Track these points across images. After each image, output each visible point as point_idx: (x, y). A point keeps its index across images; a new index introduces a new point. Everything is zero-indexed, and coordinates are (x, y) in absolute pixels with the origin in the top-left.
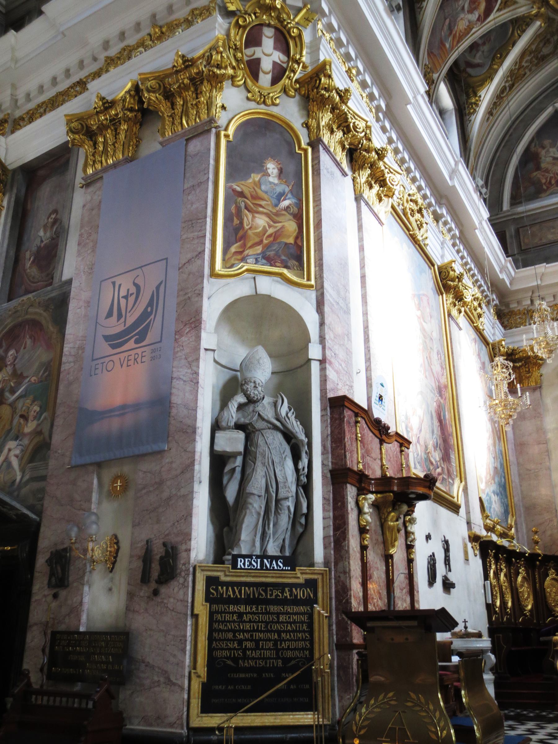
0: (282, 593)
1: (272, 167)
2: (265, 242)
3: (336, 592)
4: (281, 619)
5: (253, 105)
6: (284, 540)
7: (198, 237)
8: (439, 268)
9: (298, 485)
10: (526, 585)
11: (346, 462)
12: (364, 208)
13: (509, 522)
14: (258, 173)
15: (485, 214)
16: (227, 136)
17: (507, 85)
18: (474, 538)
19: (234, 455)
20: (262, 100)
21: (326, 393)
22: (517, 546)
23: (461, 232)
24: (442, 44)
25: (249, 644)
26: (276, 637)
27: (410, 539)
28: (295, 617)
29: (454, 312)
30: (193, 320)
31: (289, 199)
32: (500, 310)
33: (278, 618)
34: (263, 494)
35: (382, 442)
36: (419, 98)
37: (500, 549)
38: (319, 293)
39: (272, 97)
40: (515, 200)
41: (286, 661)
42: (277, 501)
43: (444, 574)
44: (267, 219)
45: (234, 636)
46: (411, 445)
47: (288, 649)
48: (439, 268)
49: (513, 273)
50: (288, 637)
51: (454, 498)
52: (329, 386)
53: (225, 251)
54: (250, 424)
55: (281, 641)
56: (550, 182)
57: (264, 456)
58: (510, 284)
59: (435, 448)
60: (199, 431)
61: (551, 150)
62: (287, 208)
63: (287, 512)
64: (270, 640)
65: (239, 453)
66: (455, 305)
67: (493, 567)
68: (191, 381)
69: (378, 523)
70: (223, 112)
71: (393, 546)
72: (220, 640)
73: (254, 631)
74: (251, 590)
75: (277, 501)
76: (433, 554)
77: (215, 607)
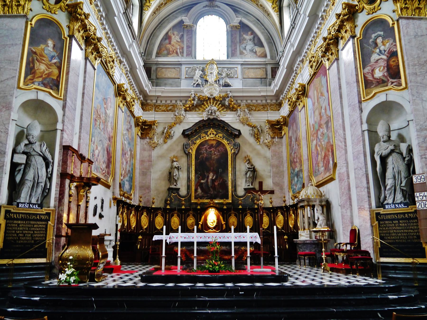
0: (36, 217)
3: (57, 217)
4: (35, 226)
5: (45, 12)
6: (38, 198)
7: (13, 69)
8: (118, 85)
9: (46, 177)
10: (134, 217)
11: (67, 170)
12: (88, 63)
13: (131, 193)
14: (44, 44)
15: (142, 64)
16: (31, 24)
17: (164, 2)
18: (115, 199)
19: (21, 164)
20: (50, 10)
21: (62, 143)
22: (133, 203)
23: (131, 69)
25: (21, 235)
26: (32, 232)
27: (88, 199)
28: (41, 226)
29: (121, 105)
30: (7, 106)
31: (56, 59)
32: (143, 102)
33: (34, 226)
34: (32, 180)
35: (81, 163)
36: (121, 15)
37: (125, 203)
38: (64, 102)
39: (55, 10)
40: (158, 54)
41: (35, 241)
42: (38, 183)
43: (100, 212)
44: (46, 67)
45: (15, 232)
46: (93, 164)
47: (37, 237)
48: (118, 85)
49: (151, 88)
50: (37, 232)
51: (108, 183)
52: (64, 140)
53: (25, 78)
54: (29, 152)
55: (34, 234)
56: (173, 51)
57: (34, 166)
58: (149, 92)
59: (103, 163)
60: (6, 153)
61: (177, 37)
62: (55, 63)
63: (41, 187)
64: (30, 234)
65: (23, 164)
66: (122, 102)
67: (121, 210)
68: (5, 132)
69: (76, 193)
71: (81, 202)
72: (9, 233)
73: (24, 230)
75: (38, 183)
76: (97, 204)
77: (8, 221)
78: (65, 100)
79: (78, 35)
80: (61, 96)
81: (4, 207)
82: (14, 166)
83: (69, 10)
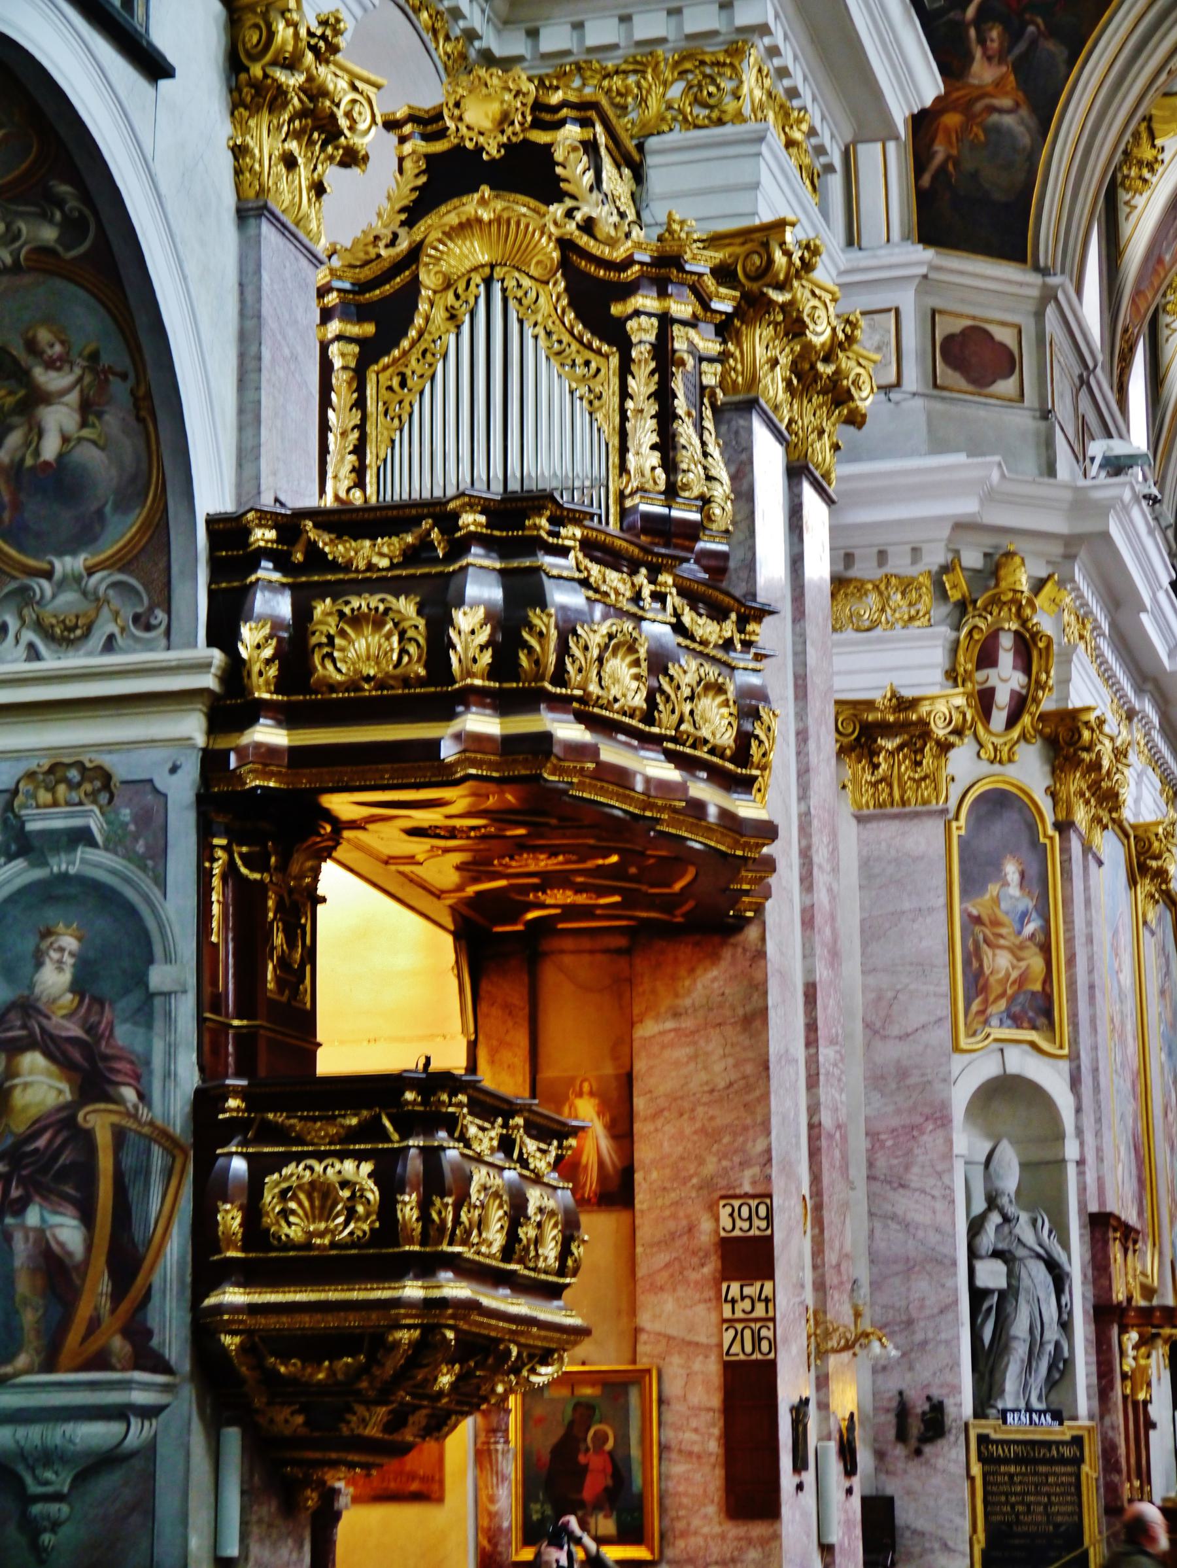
1: (1011, 870)
2: (1009, 992)
5: (985, 768)
24: (1160, 261)
25: (1020, 1508)
36: (1162, 596)
38: (1074, 1065)
41: (1057, 1526)
42: (1042, 1344)
54: (1010, 1251)
55: (1050, 1503)
57: (1027, 1291)
62: (1032, 937)
64: (1039, 1504)
70: (952, 786)
74: (1019, 1449)
75: (1042, 1344)
78: (1074, 1057)
79: (1081, 815)
80: (1061, 1047)
81: (975, 1426)
82: (977, 1295)
83: (1048, 730)
